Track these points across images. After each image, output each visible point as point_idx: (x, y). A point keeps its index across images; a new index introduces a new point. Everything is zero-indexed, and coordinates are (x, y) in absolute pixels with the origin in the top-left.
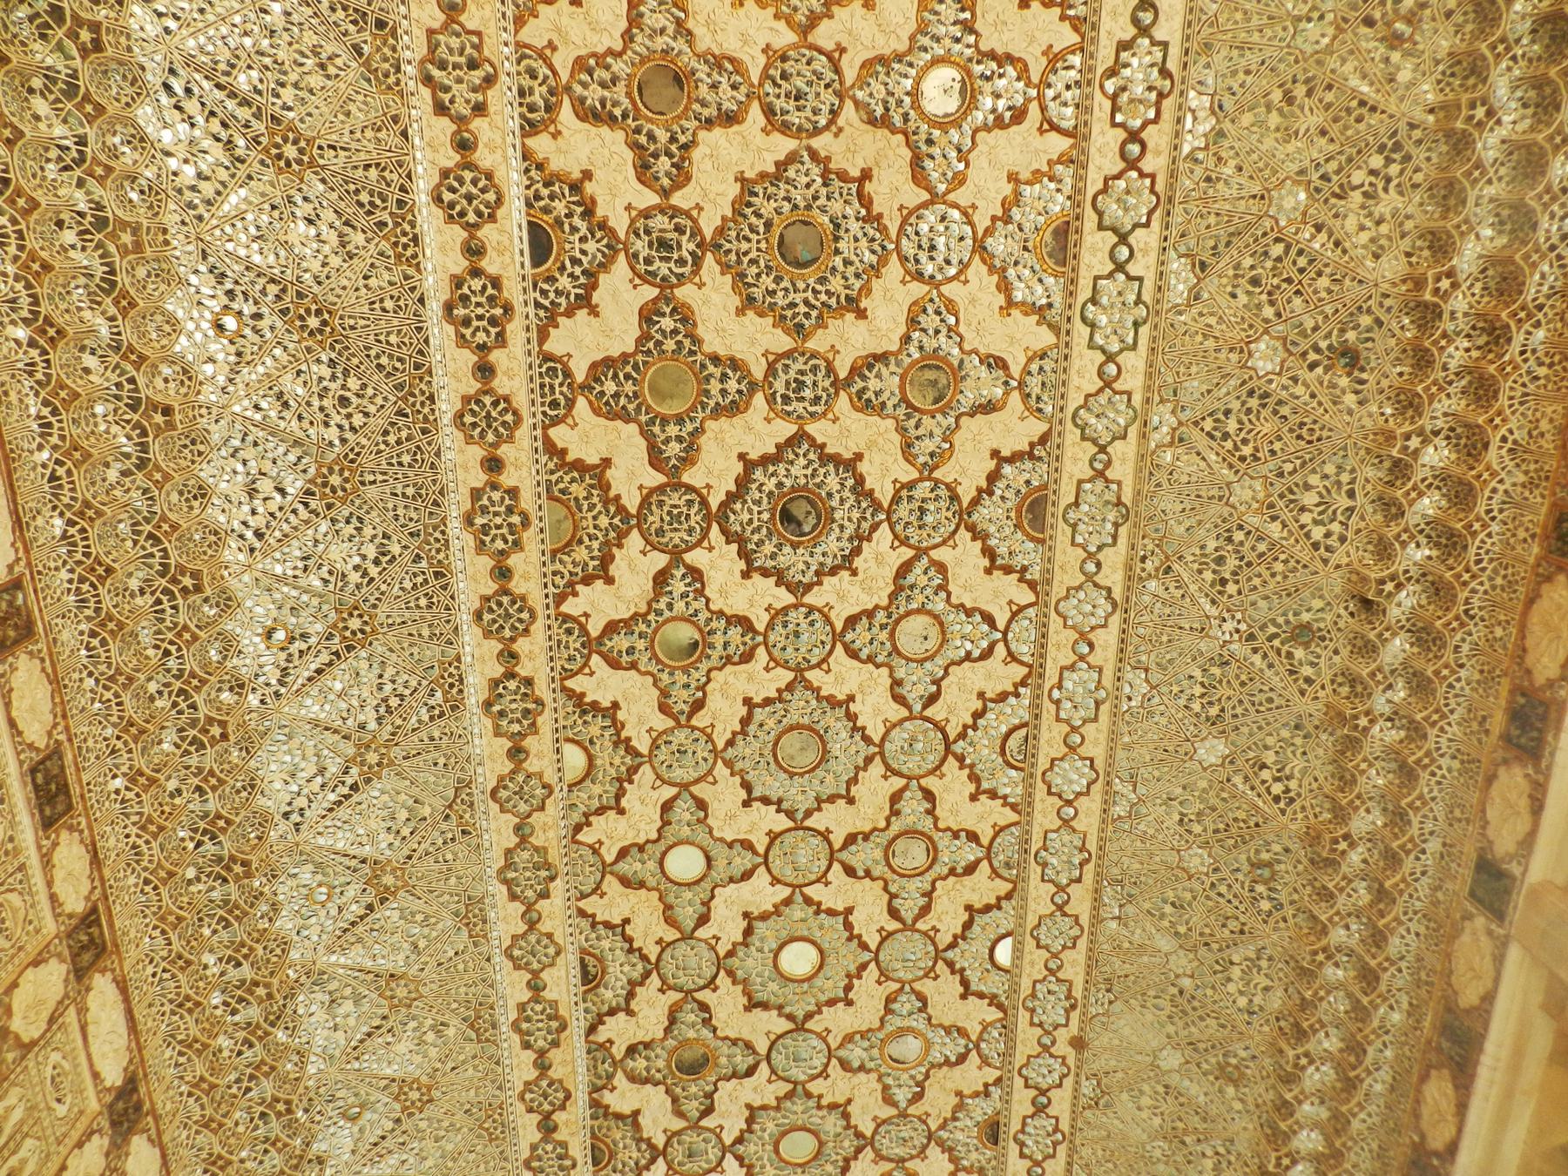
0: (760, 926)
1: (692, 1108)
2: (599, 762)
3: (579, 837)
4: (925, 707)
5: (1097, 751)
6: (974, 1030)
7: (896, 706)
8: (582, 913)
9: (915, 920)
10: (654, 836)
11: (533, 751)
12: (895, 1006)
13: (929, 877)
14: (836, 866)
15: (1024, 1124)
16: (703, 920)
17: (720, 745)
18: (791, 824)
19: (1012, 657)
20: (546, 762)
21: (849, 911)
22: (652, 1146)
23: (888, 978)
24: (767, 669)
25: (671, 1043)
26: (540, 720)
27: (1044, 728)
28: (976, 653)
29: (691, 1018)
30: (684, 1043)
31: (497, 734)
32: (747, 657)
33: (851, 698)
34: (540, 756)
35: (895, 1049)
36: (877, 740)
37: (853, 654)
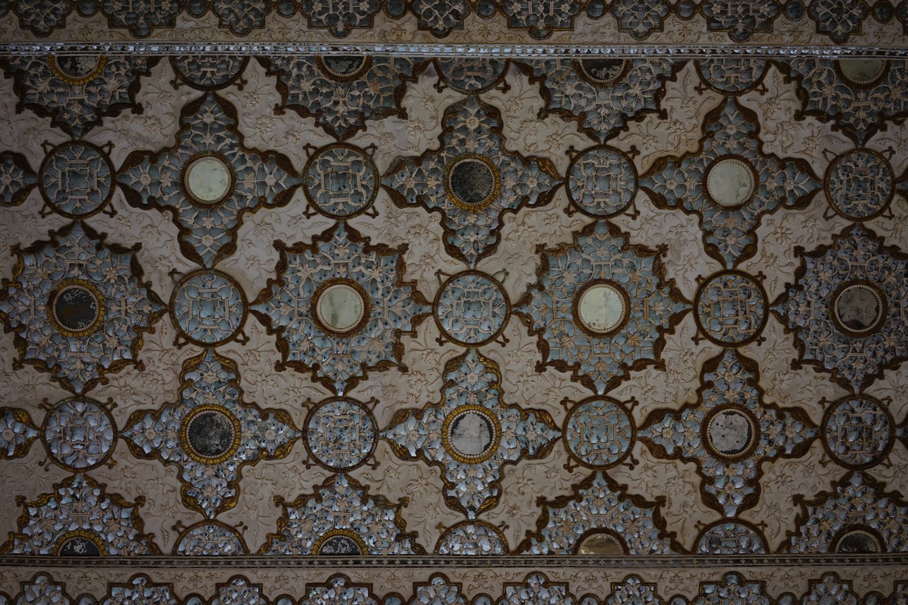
0: (646, 265)
1: (406, 180)
2: (862, 95)
3: (773, 68)
6: (496, 516)
8: (678, 66)
9: (645, 440)
10: (766, 150)
11: (886, 28)
12: (532, 418)
13: (703, 454)
14: (716, 350)
15: (359, 585)
16: (659, 201)
18: (771, 300)
21: (660, 365)
22: (351, 131)
23: (570, 413)
25: (499, 159)
27: (887, 569)
29: (532, 185)
30: (498, 174)
34: (879, 34)
35: (471, 424)
36: (869, 390)
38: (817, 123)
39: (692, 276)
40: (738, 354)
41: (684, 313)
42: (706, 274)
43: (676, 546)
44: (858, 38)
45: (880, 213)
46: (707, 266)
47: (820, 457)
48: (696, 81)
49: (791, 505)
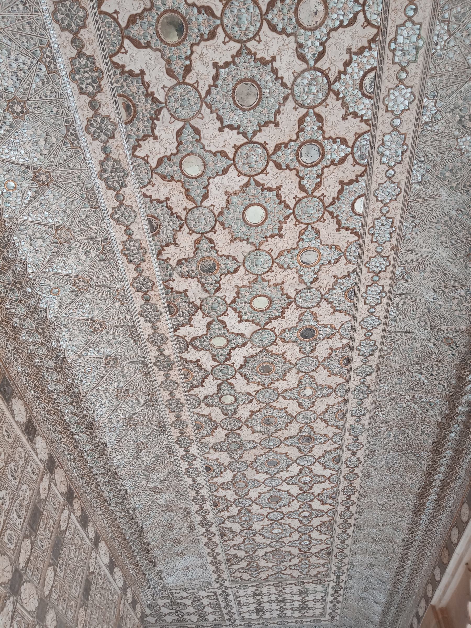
0: (234, 199)
1: (211, 288)
2: (139, 108)
3: (136, 153)
4: (316, 61)
5: (416, 81)
6: (343, 245)
7: (300, 62)
8: (145, 195)
9: (313, 191)
10: (174, 151)
11: (103, 103)
12: (303, 237)
13: (320, 166)
14: (271, 164)
15: (367, 290)
16: (206, 196)
17: (203, 95)
18: (246, 140)
19: (368, 22)
20: (110, 109)
21: (279, 188)
22: (195, 305)
23: (300, 223)
24: (225, 43)
25: (197, 259)
26: (103, 83)
27: (385, 68)
28: (346, 23)
30: (203, 259)
31: (81, 93)
32: (212, 35)
33: (274, 59)
34: (106, 105)
35: (306, 257)
36: (289, 85)
37: (273, 28)
38: (157, 128)
39: (238, 179)
40: (273, 154)
41: (255, 180)
42: (236, 172)
43: (362, 175)
44: (112, 117)
45: (196, 89)
46: (233, 172)
47: (324, 108)
48: (149, 187)
49: (347, 121)
